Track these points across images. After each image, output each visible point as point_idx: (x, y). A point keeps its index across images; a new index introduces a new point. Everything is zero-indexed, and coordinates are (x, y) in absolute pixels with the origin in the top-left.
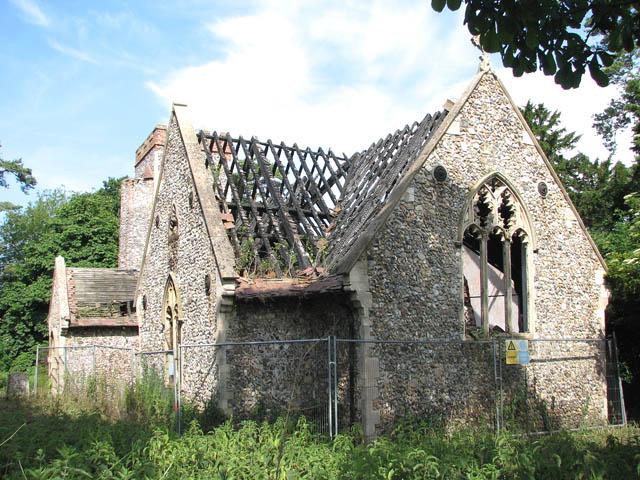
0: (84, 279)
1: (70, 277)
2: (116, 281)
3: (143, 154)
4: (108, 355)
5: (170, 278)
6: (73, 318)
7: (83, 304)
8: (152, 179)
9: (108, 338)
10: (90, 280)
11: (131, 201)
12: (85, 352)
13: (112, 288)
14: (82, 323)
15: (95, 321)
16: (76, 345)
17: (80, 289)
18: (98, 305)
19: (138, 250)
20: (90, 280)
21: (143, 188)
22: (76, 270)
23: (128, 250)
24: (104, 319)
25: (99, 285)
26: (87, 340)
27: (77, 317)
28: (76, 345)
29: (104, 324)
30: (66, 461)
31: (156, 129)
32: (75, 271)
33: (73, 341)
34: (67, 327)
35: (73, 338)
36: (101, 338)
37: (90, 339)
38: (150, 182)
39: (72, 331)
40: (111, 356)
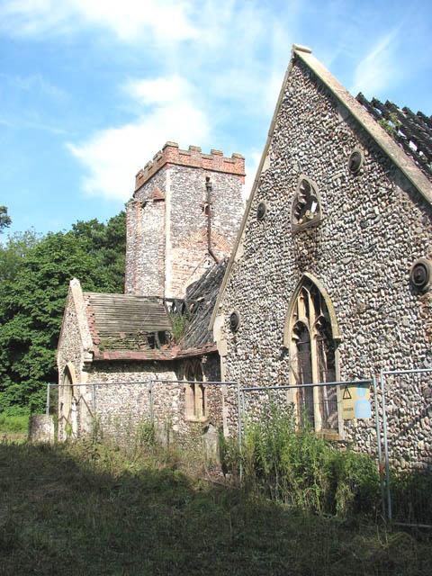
0: (103, 305)
1: (87, 303)
2: (140, 308)
3: (146, 176)
4: (136, 394)
5: (307, 281)
6: (97, 351)
7: (105, 334)
8: (163, 200)
9: (136, 373)
10: (111, 307)
11: (139, 225)
12: (110, 391)
13: (136, 317)
14: (107, 356)
15: (122, 354)
16: (100, 381)
17: (101, 317)
18: (123, 336)
19: (148, 278)
20: (111, 307)
21: (154, 211)
22: (93, 295)
23: (137, 279)
24: (131, 352)
25: (123, 312)
26: (112, 377)
27: (101, 349)
28: (100, 381)
29: (132, 357)
30: (335, 542)
31: (166, 146)
32: (92, 297)
33: (97, 377)
34: (91, 360)
35: (96, 373)
36: (128, 374)
37: (115, 375)
38: (161, 203)
39: (97, 365)
40: (139, 396)
